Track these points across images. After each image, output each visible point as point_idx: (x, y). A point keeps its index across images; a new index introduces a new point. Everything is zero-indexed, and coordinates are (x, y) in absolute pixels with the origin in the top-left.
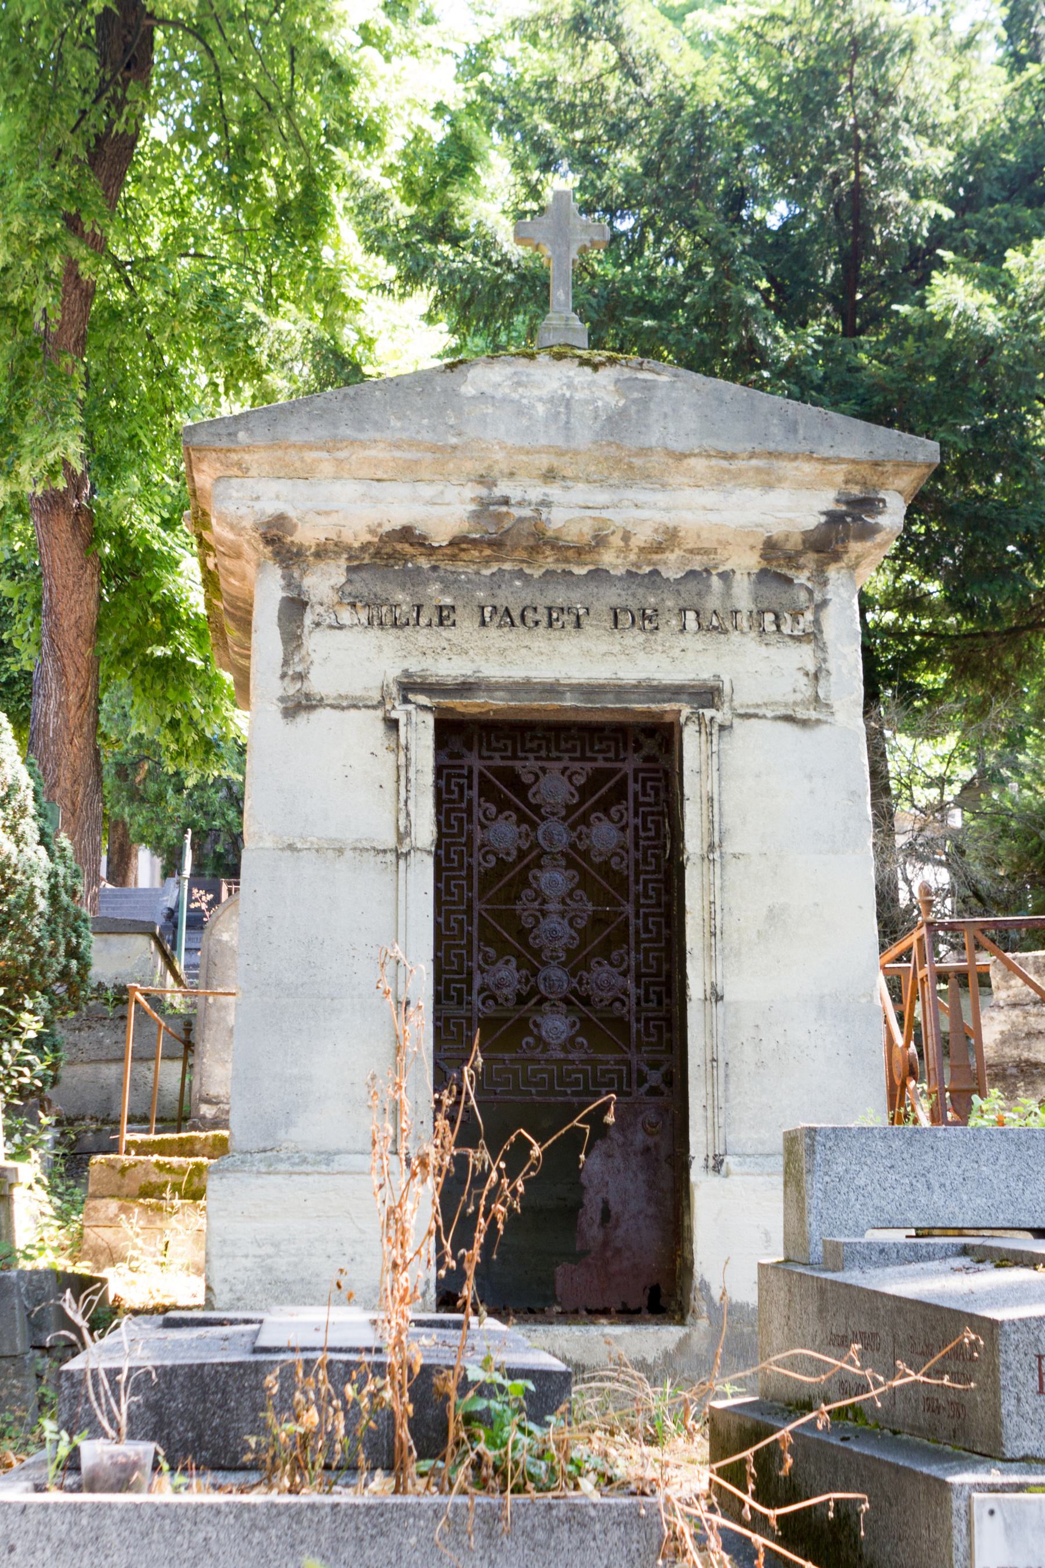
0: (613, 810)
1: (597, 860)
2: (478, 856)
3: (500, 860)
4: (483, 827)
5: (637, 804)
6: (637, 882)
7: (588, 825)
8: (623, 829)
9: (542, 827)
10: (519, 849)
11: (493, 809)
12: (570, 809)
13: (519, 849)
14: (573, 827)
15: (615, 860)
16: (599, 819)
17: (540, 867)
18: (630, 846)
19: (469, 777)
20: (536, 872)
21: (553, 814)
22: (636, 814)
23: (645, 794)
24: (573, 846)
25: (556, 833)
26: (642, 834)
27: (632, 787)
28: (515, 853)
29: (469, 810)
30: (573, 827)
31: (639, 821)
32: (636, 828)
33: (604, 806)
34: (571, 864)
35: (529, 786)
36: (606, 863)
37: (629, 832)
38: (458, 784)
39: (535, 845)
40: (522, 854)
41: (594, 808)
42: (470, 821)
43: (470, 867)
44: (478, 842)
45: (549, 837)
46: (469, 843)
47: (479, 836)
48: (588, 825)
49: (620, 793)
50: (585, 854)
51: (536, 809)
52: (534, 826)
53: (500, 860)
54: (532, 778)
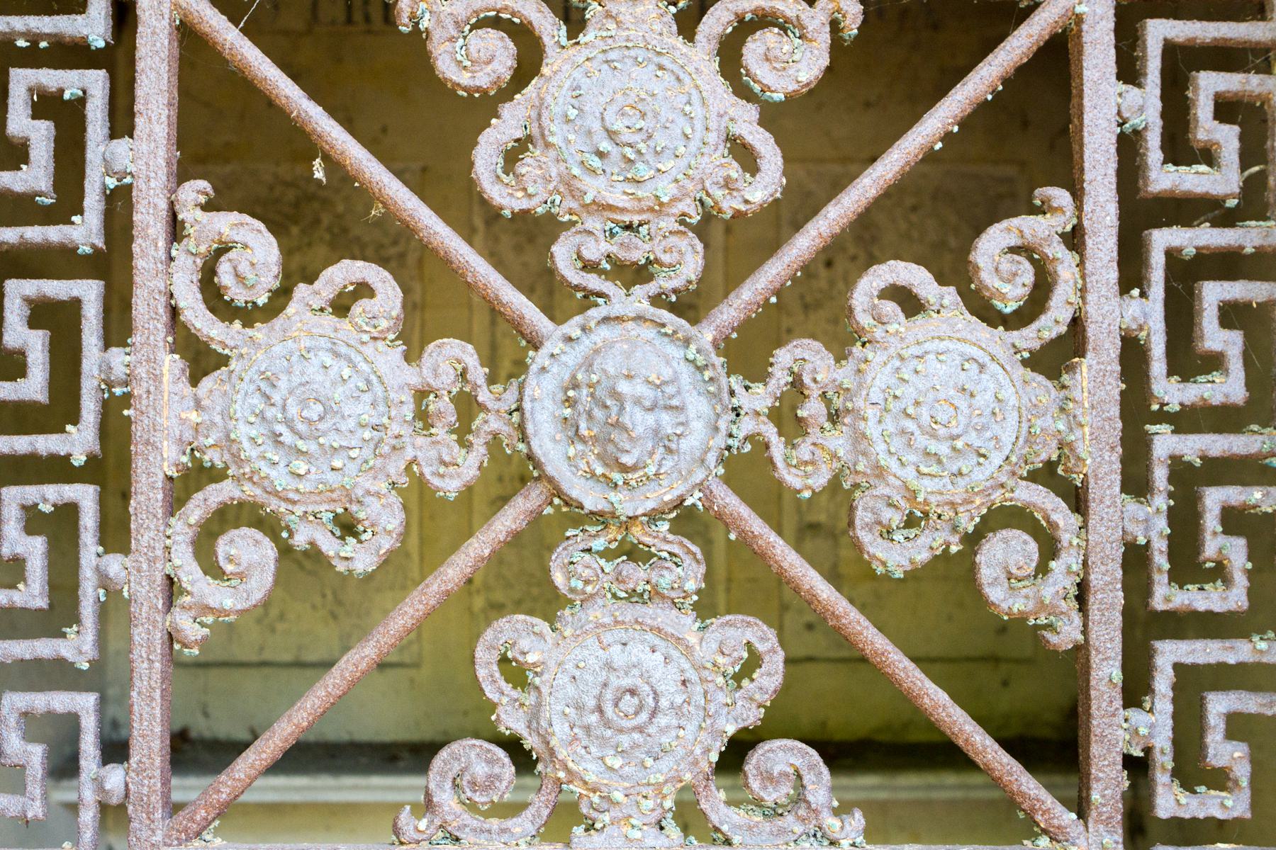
0: (991, 247)
1: (897, 556)
2: (162, 537)
3: (299, 564)
4: (201, 361)
5: (1141, 213)
6: (1135, 691)
7: (844, 339)
8: (1056, 359)
9: (559, 353)
10: (417, 494)
11: (256, 252)
12: (733, 242)
13: (417, 494)
14: (746, 354)
15: (1007, 552)
16: (910, 303)
17: (547, 603)
18: (1100, 463)
19: (117, 60)
20: (519, 633)
21: (634, 274)
22: (1131, 276)
23: (1180, 147)
24: (748, 469)
25: (639, 396)
26: (1170, 391)
27: (1109, 104)
28: (386, 519)
29: (111, 265)
30: (746, 354)
31: (1148, 313)
32: (1133, 353)
33: (939, 220)
34: (737, 584)
35: (484, 106)
36: (956, 570)
37: (1097, 375)
38: (46, 104)
39: (514, 470)
40: (433, 520)
41: (866, 241)
42: (118, 328)
43: (114, 607)
44: (156, 462)
45: (595, 415)
46: (110, 469)
47: (171, 418)
48: (844, 339)
49: (1032, 131)
50: (823, 527)
51: (523, 241)
52: (507, 352)
53: (299, 564)
54: (498, 54)
